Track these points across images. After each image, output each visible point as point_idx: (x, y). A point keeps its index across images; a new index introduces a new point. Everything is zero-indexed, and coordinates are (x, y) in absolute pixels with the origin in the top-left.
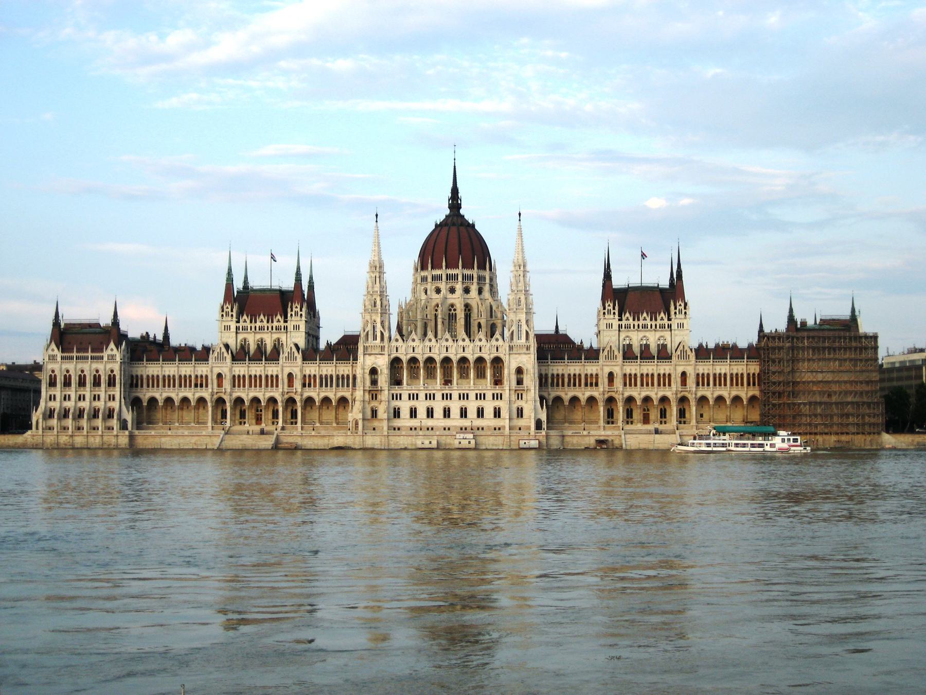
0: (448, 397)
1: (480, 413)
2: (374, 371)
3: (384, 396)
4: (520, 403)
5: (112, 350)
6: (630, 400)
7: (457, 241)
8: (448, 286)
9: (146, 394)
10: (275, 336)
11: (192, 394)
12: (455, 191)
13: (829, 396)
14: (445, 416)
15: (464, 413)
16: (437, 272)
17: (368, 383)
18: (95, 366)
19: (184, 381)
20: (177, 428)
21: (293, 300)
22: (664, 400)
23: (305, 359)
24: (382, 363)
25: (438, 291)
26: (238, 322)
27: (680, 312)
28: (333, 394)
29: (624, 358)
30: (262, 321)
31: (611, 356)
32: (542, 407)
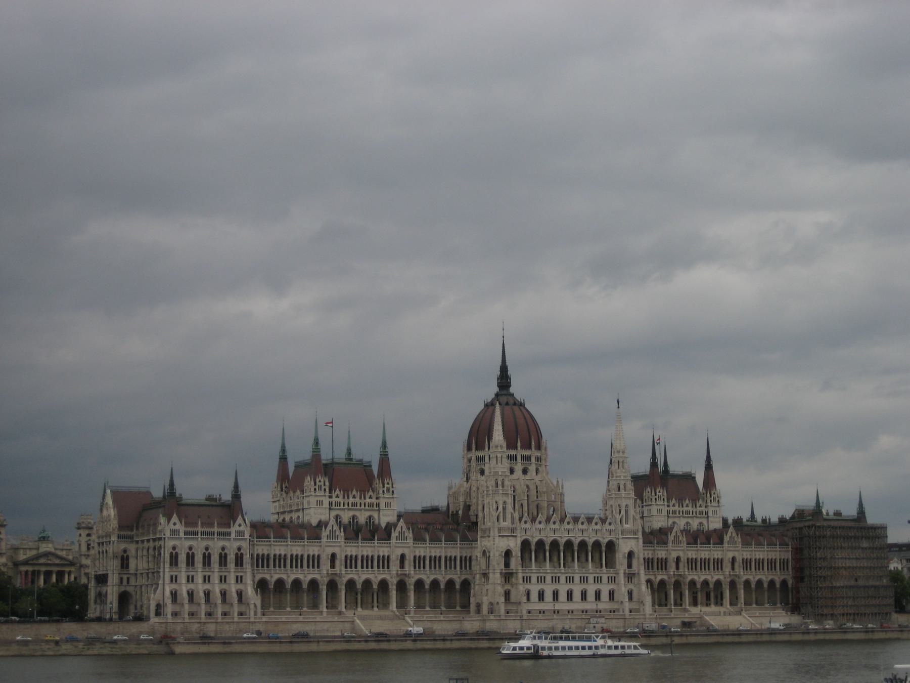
1: (598, 595)
4: (631, 586)
5: (240, 525)
6: (693, 583)
10: (368, 514)
11: (305, 576)
12: (504, 369)
13: (856, 580)
16: (512, 452)
17: (503, 567)
18: (221, 544)
19: (297, 561)
20: (290, 613)
21: (355, 476)
22: (718, 583)
23: (414, 540)
24: (514, 545)
25: (512, 471)
26: (330, 497)
28: (443, 577)
31: (676, 541)
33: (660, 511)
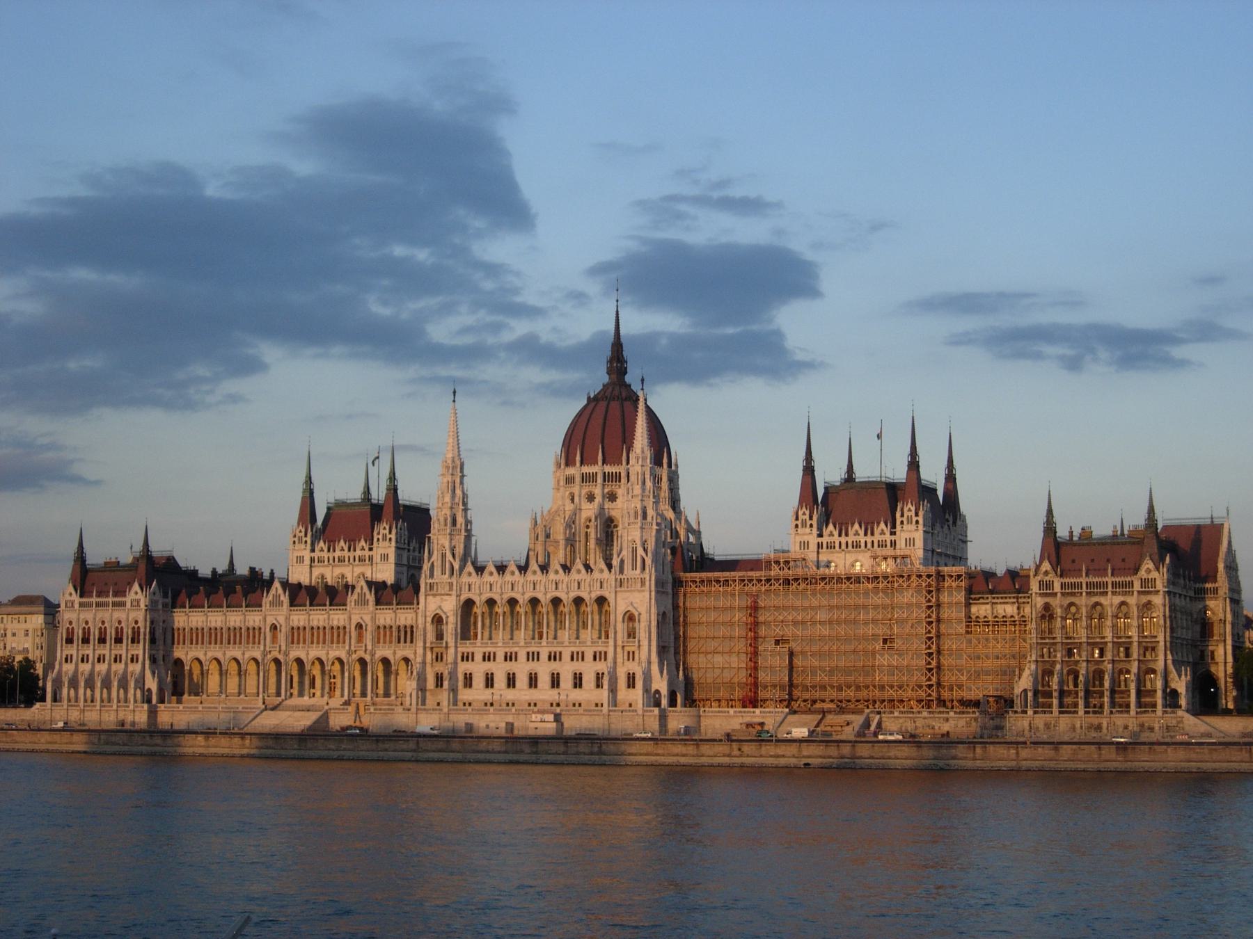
0: (533, 656)
2: (438, 620)
3: (450, 656)
7: (601, 421)
8: (584, 492)
10: (358, 570)
14: (531, 686)
15: (555, 681)
17: (431, 637)
19: (234, 636)
23: (378, 602)
24: (449, 606)
26: (313, 550)
27: (910, 521)
30: (342, 549)
32: (662, 673)
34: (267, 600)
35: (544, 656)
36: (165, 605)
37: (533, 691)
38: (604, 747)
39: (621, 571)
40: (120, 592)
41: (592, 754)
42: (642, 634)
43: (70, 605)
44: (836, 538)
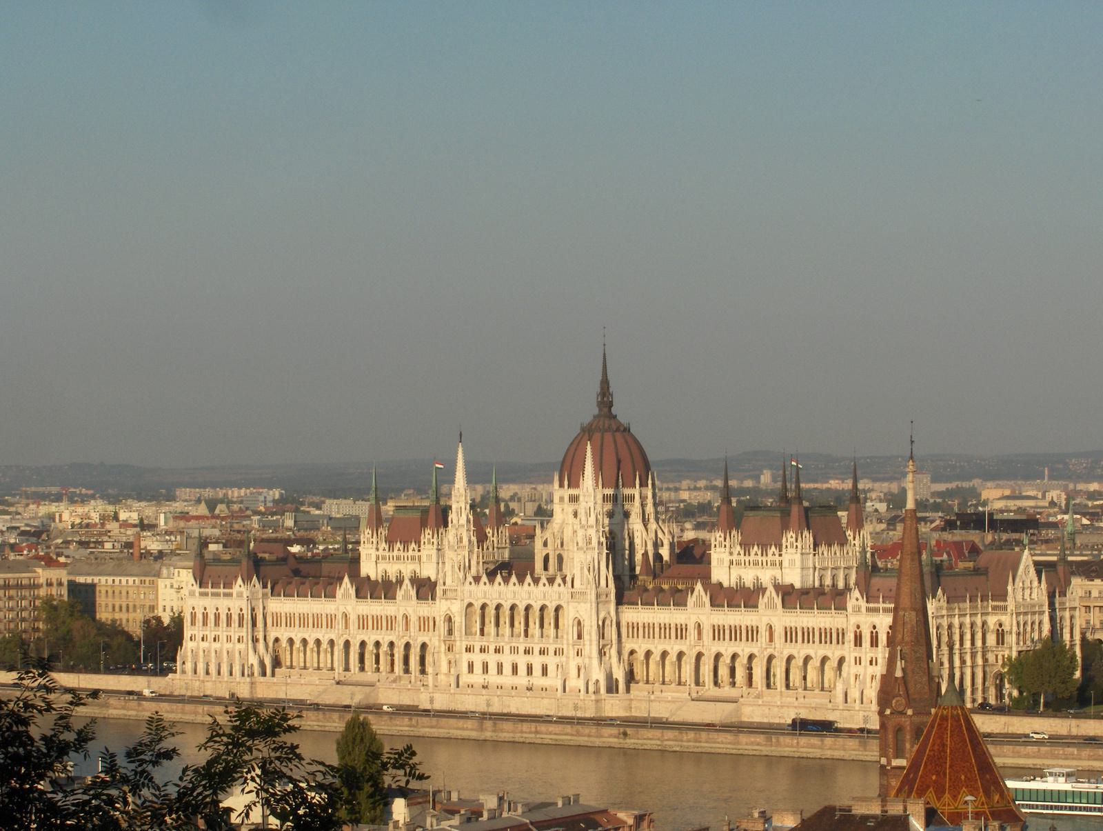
0: (514, 650)
9: (284, 634)
12: (605, 383)
19: (317, 621)
24: (456, 609)
26: (377, 549)
27: (792, 545)
29: (712, 605)
31: (699, 604)
33: (721, 561)
34: (340, 592)
35: (521, 650)
36: (264, 595)
37: (515, 677)
38: (538, 728)
39: (573, 586)
40: (228, 585)
41: (531, 733)
42: (586, 636)
43: (192, 594)
44: (742, 557)
